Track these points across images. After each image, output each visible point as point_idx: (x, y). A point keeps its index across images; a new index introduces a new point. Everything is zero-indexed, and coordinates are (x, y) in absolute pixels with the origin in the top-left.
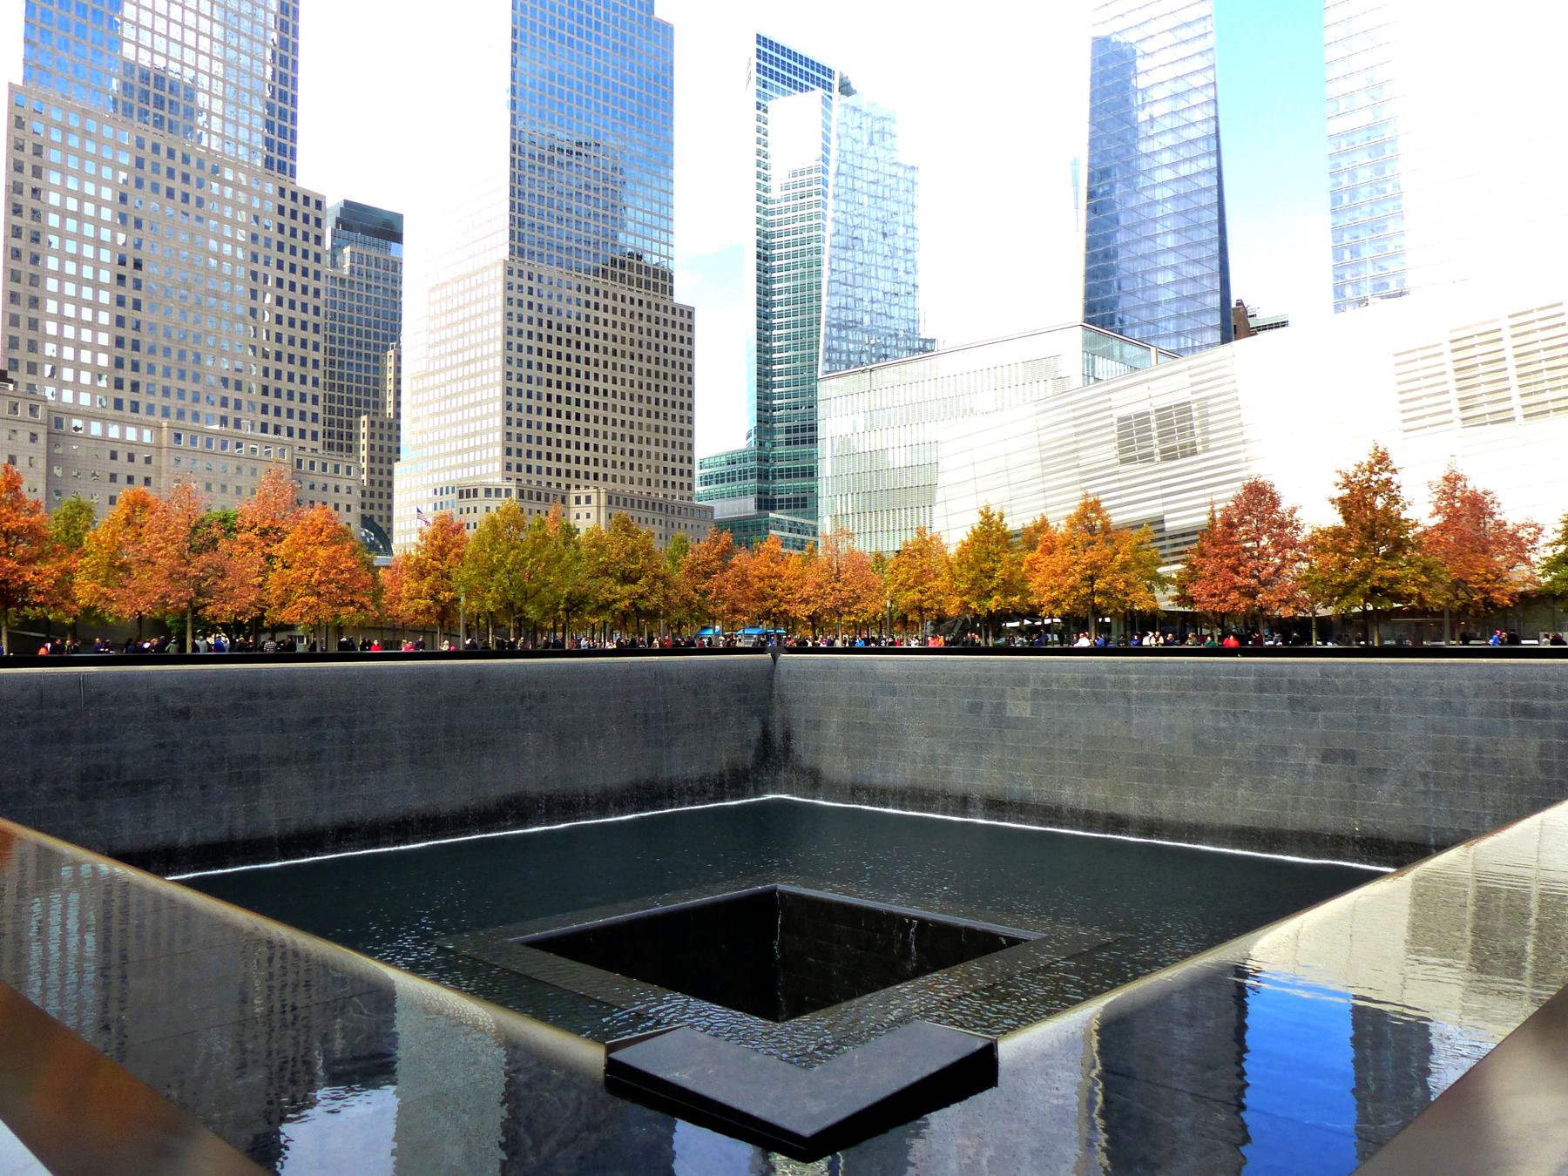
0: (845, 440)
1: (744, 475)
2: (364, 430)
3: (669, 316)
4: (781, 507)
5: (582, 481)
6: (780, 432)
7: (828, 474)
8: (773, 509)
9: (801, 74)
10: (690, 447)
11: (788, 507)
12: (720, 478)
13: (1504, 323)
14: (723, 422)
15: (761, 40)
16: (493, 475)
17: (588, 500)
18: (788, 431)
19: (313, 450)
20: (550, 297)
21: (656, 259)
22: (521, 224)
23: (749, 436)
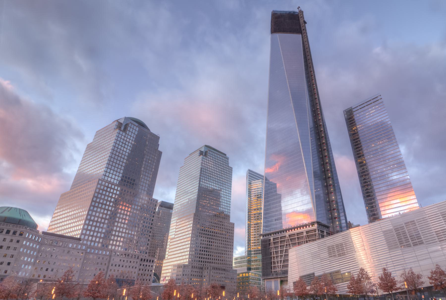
3: (229, 225)
5: (207, 264)
9: (257, 177)
12: (239, 262)
13: (404, 225)
17: (208, 268)
21: (227, 213)
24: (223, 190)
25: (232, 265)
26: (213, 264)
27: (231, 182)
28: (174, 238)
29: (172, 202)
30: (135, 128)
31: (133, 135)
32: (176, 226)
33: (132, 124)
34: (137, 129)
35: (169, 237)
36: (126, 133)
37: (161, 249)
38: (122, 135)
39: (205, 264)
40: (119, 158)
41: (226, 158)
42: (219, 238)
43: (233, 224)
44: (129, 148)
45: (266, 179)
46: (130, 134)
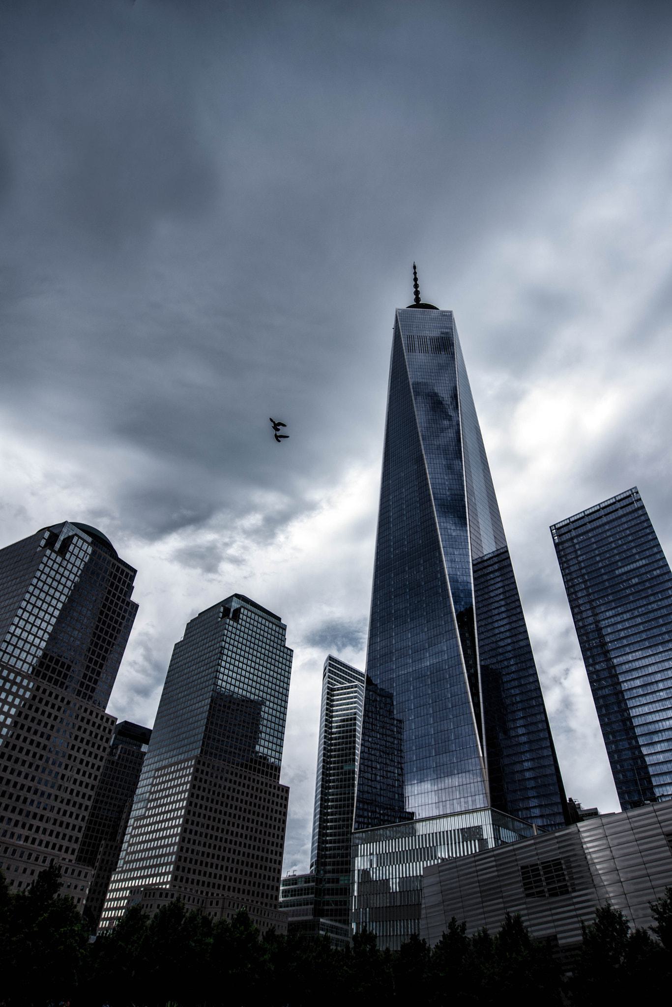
0: (365, 873)
1: (306, 891)
2: (101, 849)
3: (276, 791)
4: (327, 916)
6: (329, 865)
7: (356, 894)
8: (322, 916)
10: (279, 872)
11: (331, 915)
12: (293, 893)
14: (298, 858)
15: (330, 658)
16: (166, 883)
17: (217, 904)
18: (334, 865)
19: (70, 861)
20: (217, 777)
21: (273, 760)
22: (209, 738)
23: (311, 866)
24: (268, 703)
25: (277, 898)
26: (231, 894)
27: (288, 684)
28: (144, 817)
29: (150, 725)
30: (85, 546)
31: (78, 563)
32: (153, 785)
33: (80, 537)
34: (90, 551)
35: (133, 814)
36: (64, 558)
37: (110, 843)
38: (54, 561)
39: (211, 890)
40: (42, 614)
41: (280, 627)
42: (250, 825)
43: (286, 790)
44: (66, 591)
45: (369, 681)
46: (73, 559)
